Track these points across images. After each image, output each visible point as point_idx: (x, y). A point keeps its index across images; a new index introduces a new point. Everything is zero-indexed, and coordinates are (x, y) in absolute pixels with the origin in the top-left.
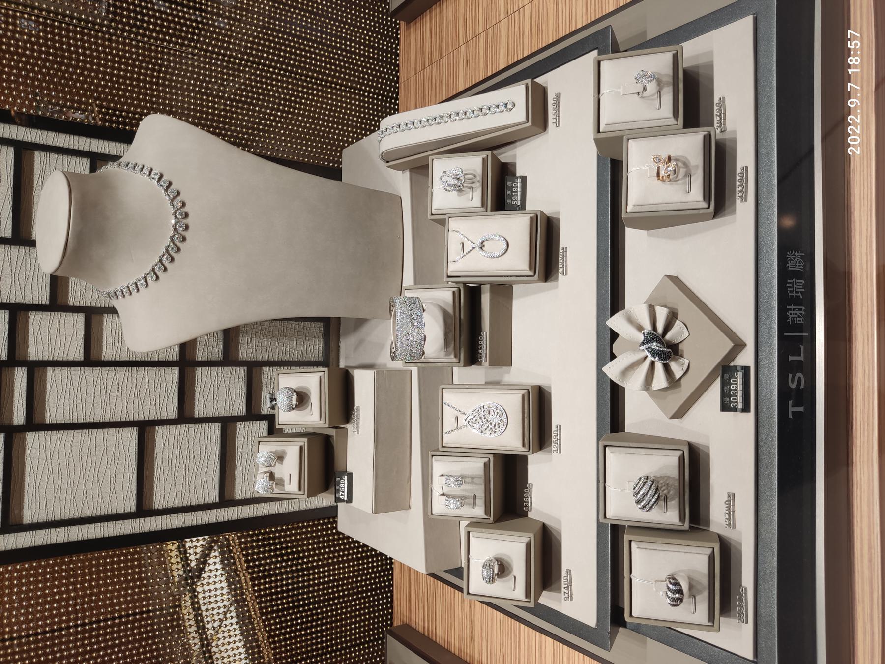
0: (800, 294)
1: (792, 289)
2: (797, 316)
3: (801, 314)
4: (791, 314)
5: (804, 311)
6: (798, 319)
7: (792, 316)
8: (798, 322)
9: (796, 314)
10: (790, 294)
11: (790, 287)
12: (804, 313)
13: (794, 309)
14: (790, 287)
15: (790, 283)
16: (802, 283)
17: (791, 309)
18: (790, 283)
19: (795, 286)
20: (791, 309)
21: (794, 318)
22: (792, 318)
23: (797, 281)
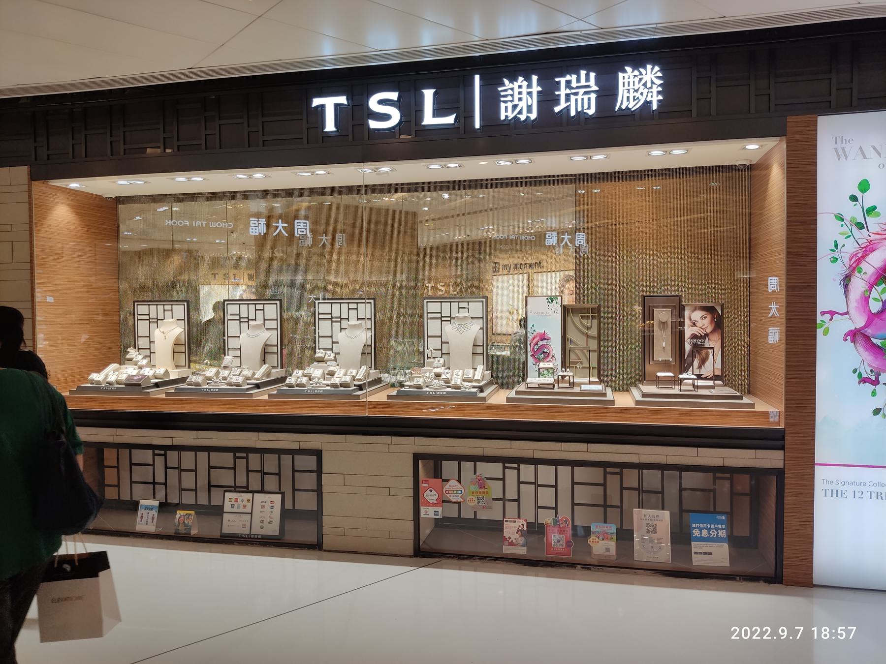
0: (563, 105)
1: (574, 84)
2: (516, 102)
3: (520, 113)
4: (520, 87)
5: (528, 117)
6: (510, 105)
7: (517, 90)
8: (503, 105)
9: (520, 99)
10: (563, 80)
11: (578, 80)
12: (523, 117)
13: (530, 93)
14: (578, 80)
15: (588, 79)
16: (589, 108)
17: (529, 86)
18: (588, 79)
19: (582, 91)
20: (529, 86)
21: (512, 95)
22: (512, 89)
23: (593, 96)
